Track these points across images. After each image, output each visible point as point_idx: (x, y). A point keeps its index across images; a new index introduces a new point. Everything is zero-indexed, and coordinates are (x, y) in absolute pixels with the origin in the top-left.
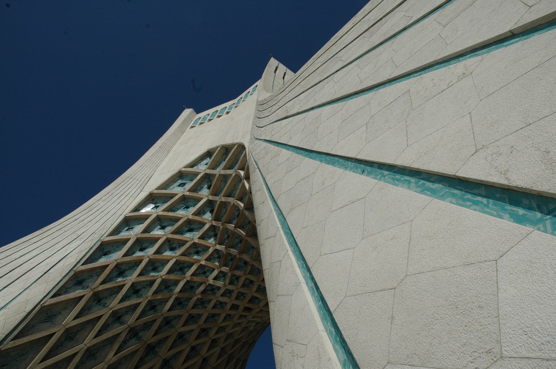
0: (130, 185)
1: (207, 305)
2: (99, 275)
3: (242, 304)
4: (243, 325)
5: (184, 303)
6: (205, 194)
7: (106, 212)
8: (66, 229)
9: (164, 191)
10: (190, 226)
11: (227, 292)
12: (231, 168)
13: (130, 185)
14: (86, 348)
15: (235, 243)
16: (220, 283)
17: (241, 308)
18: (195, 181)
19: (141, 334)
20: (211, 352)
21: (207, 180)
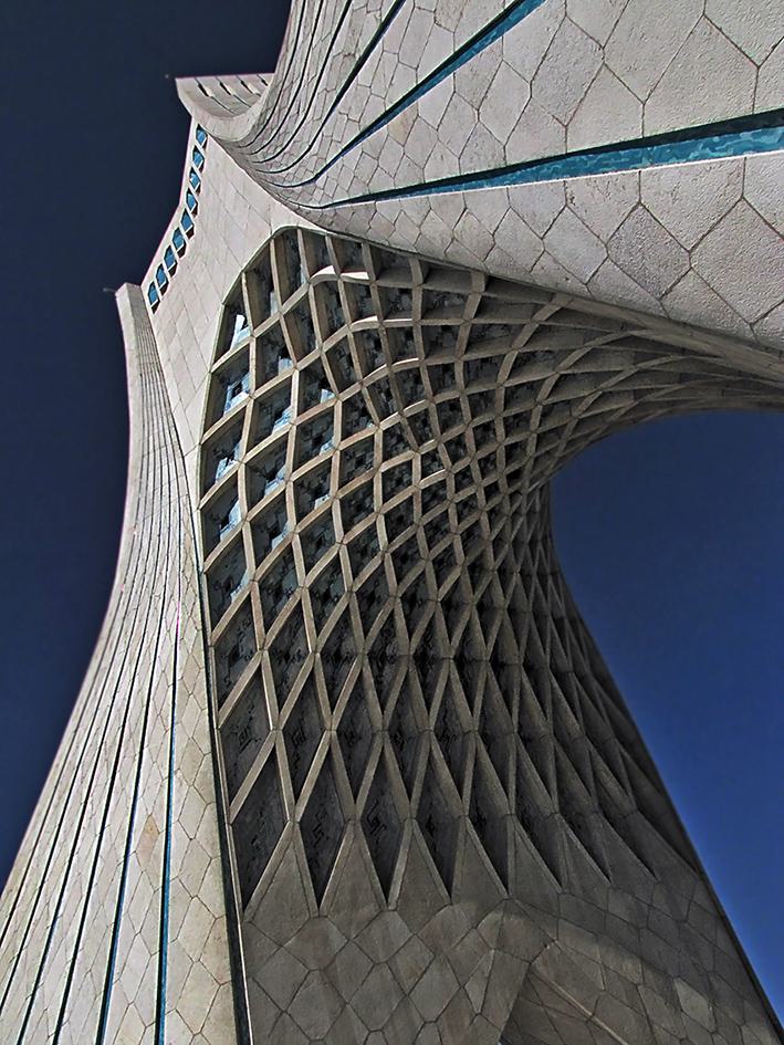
0: (158, 465)
1: (446, 526)
2: (251, 623)
3: (498, 476)
4: (524, 511)
5: (410, 553)
6: (290, 370)
7: (164, 531)
8: (133, 605)
9: (219, 424)
10: (312, 436)
11: (460, 478)
12: (295, 285)
13: (158, 465)
14: (334, 733)
15: (409, 392)
16: (436, 476)
17: (503, 482)
18: (253, 364)
19: (389, 651)
20: (510, 591)
21: (269, 346)
